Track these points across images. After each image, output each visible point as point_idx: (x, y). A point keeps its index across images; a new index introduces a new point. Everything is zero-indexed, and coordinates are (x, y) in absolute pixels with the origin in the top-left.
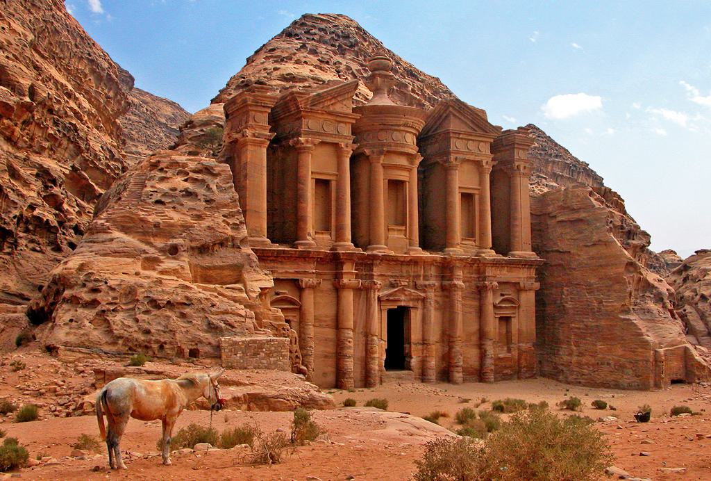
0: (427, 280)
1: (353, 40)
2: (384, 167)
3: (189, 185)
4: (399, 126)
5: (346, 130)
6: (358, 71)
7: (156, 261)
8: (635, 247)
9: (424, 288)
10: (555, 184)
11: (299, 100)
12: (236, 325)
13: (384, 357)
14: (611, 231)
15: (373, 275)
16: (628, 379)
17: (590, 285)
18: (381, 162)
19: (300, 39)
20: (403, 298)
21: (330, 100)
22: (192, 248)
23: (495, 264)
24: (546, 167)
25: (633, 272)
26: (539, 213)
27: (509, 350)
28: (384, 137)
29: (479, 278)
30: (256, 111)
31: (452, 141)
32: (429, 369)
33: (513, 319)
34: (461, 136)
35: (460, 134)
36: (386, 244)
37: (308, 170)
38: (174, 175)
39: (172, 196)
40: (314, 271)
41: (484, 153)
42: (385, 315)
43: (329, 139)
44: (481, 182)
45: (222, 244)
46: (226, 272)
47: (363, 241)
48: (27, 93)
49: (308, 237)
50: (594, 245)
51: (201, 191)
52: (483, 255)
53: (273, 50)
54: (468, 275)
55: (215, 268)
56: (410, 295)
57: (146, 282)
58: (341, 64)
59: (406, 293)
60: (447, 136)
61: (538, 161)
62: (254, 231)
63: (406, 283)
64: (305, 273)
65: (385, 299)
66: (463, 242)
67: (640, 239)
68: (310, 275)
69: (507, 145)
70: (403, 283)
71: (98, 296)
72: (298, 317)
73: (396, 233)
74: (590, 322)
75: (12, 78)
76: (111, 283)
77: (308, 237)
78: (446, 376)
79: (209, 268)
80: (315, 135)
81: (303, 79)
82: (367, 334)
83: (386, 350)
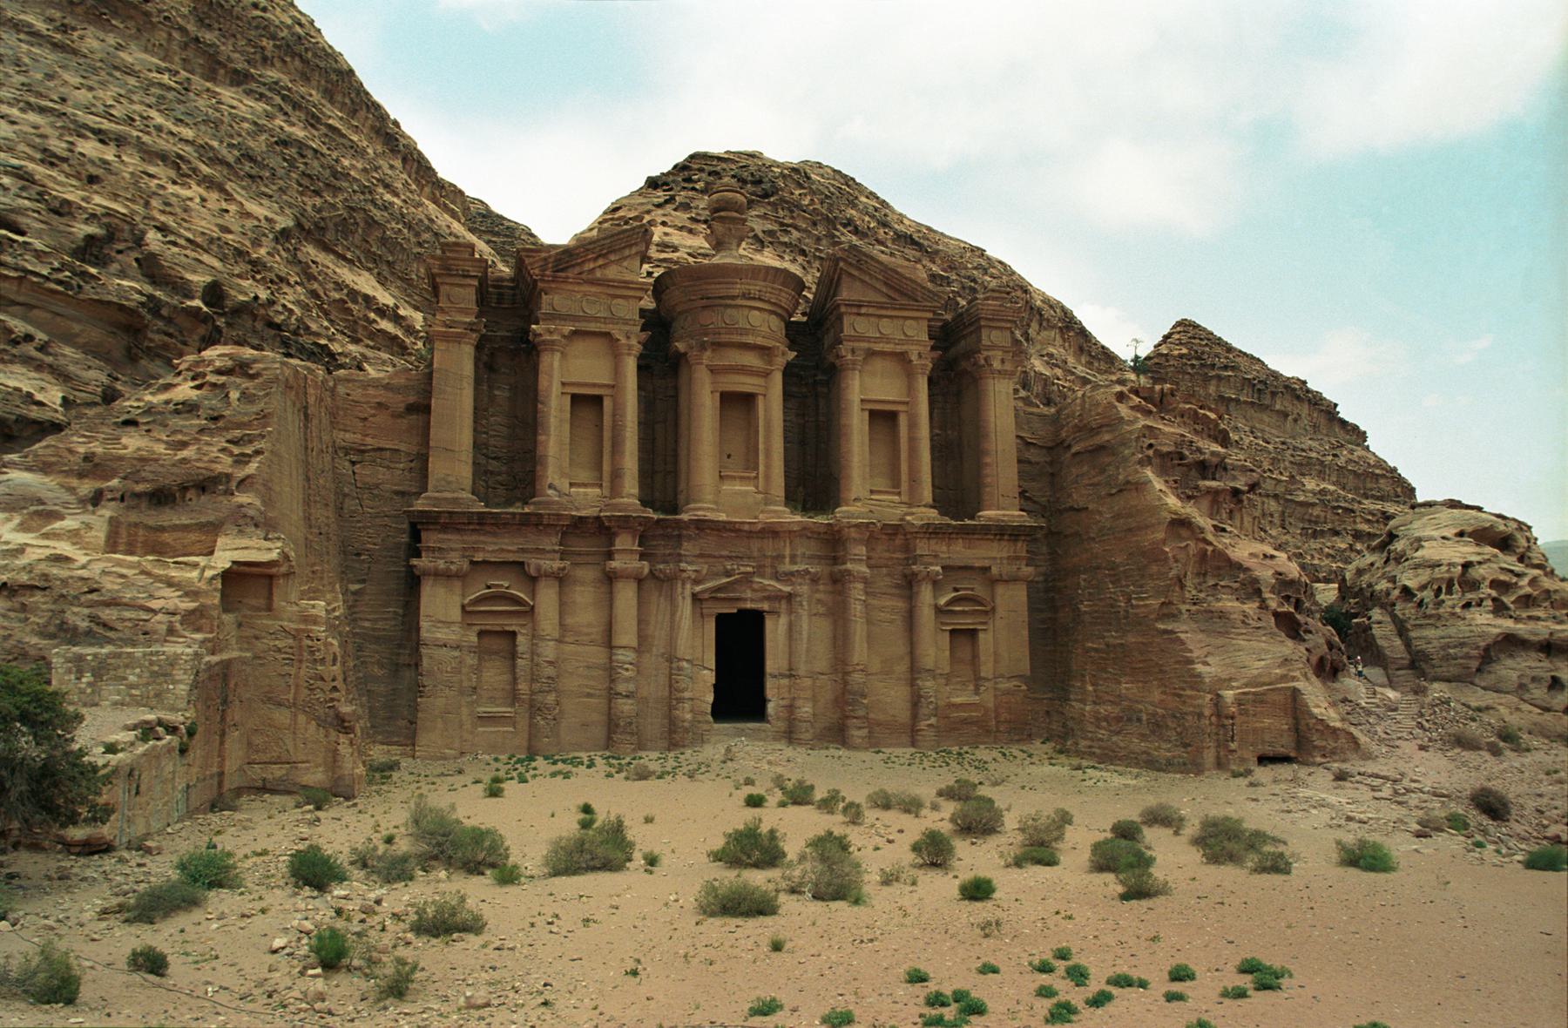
0: (795, 563)
1: (767, 186)
2: (712, 371)
4: (733, 298)
6: (771, 233)
8: (1215, 494)
9: (788, 577)
11: (527, 261)
12: (119, 626)
13: (710, 698)
14: (1150, 463)
15: (680, 555)
16: (1169, 750)
17: (1113, 567)
19: (671, 189)
20: (749, 594)
21: (595, 259)
22: (138, 495)
23: (932, 531)
24: (1205, 388)
25: (1188, 539)
26: (1050, 444)
27: (977, 692)
28: (712, 319)
29: (907, 559)
30: (452, 284)
31: (846, 321)
33: (981, 636)
34: (863, 310)
35: (860, 306)
36: (716, 503)
37: (551, 376)
38: (185, 380)
40: (557, 548)
41: (914, 335)
43: (593, 327)
46: (193, 537)
47: (682, 497)
48: (199, 294)
49: (550, 492)
50: (1120, 491)
52: (908, 518)
54: (887, 555)
55: (175, 528)
56: (764, 589)
61: (1187, 377)
62: (443, 483)
63: (749, 569)
64: (538, 551)
65: (706, 596)
67: (1234, 478)
68: (548, 556)
69: (971, 325)
70: (743, 569)
72: (530, 625)
73: (738, 481)
74: (1113, 637)
75: (173, 272)
78: (836, 734)
79: (162, 529)
82: (671, 658)
83: (715, 686)
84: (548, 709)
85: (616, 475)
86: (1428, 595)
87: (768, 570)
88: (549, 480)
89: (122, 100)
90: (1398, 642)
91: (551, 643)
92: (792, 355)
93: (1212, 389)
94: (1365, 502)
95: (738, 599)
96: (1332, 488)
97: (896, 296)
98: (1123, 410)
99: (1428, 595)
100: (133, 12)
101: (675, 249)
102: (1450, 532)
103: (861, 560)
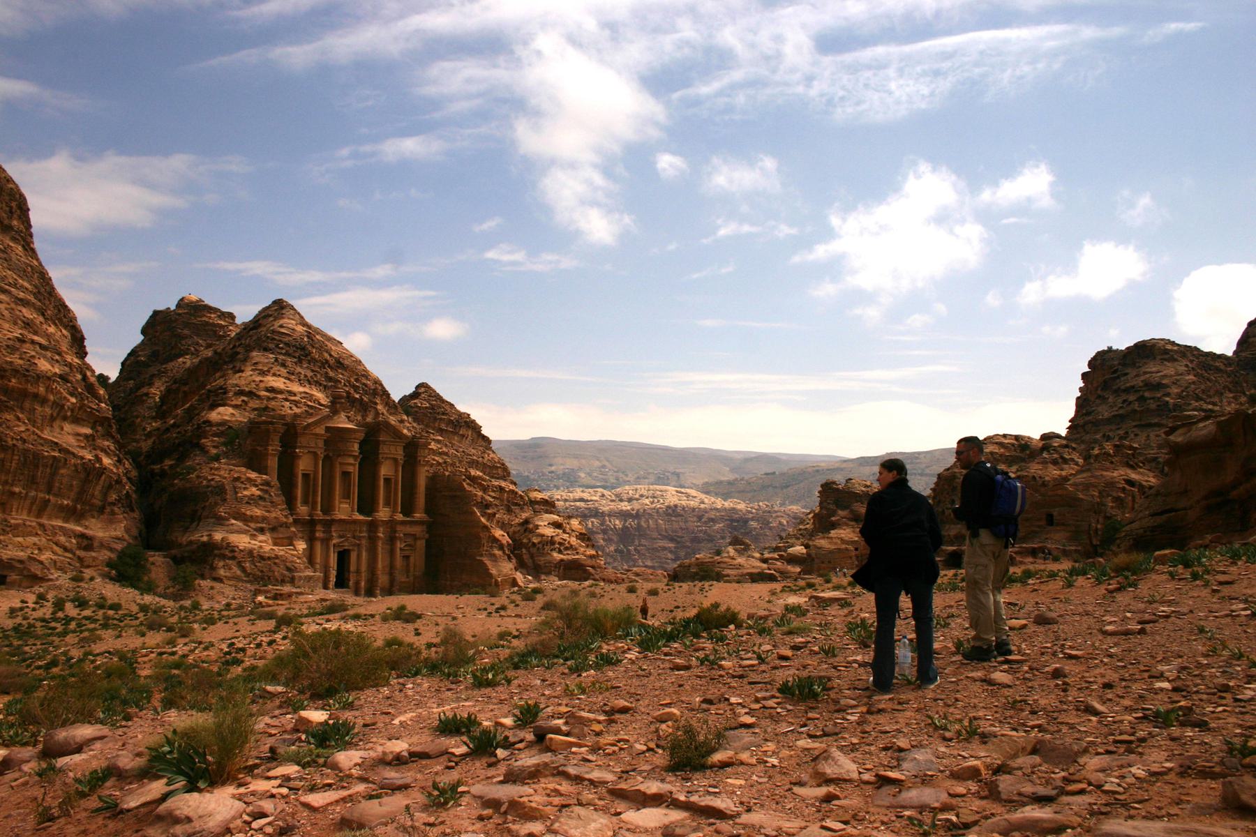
3: (259, 493)
5: (321, 444)
6: (311, 377)
7: (255, 535)
8: (489, 514)
9: (360, 538)
10: (440, 438)
23: (403, 523)
27: (408, 577)
31: (381, 446)
39: (252, 499)
41: (399, 453)
42: (336, 555)
44: (396, 471)
45: (281, 526)
51: (266, 496)
53: (256, 363)
57: (256, 547)
58: (300, 373)
60: (378, 443)
71: (236, 554)
76: (241, 548)
78: (370, 593)
79: (276, 539)
81: (281, 392)
85: (315, 503)
86: (540, 546)
90: (531, 561)
93: (437, 425)
94: (493, 480)
96: (481, 474)
98: (464, 484)
99: (540, 546)
101: (295, 395)
102: (546, 523)
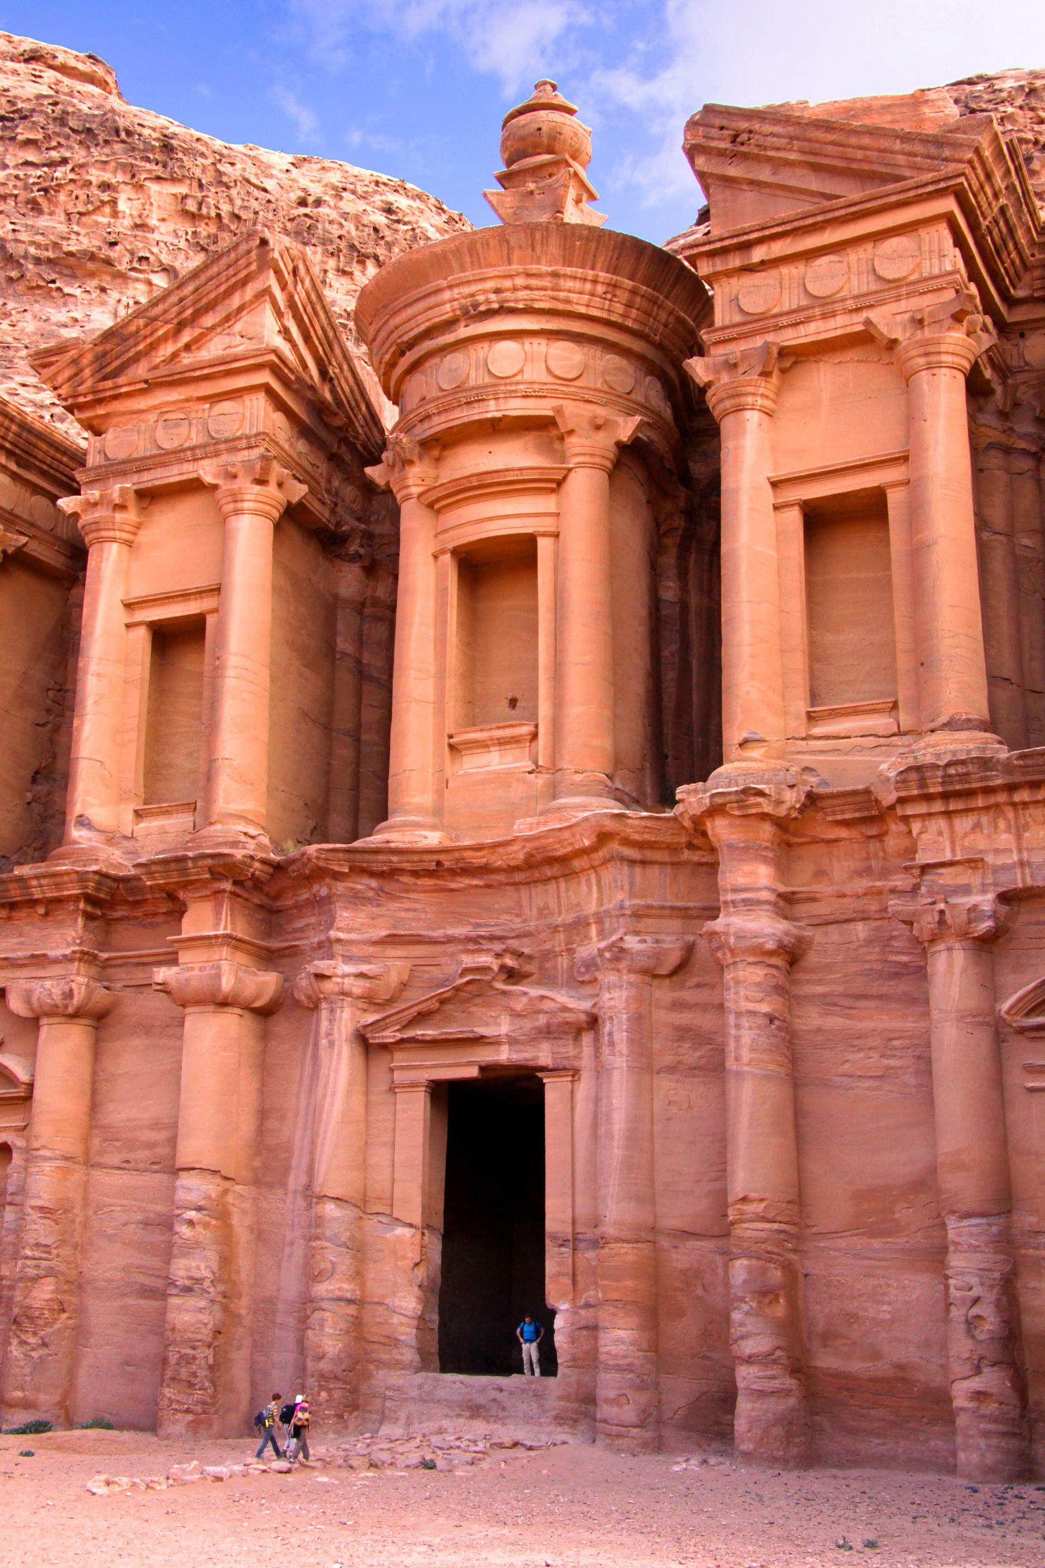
2: (430, 506)
4: (450, 324)
15: (330, 942)
18: (415, 490)
31: (719, 294)
32: (607, 1368)
34: (758, 254)
35: (747, 246)
36: (438, 811)
40: (68, 951)
43: (174, 474)
59: (519, 1005)
63: (484, 959)
65: (390, 1035)
66: (816, 731)
68: (58, 970)
70: (468, 961)
77: (76, 833)
80: (124, 474)
82: (312, 1196)
84: (31, 1319)
87: (563, 962)
88: (78, 809)
89: (21, 391)
91: (47, 1166)
92: (626, 428)
95: (478, 1041)
97: (829, 186)
100: (91, 266)
103: (759, 902)
